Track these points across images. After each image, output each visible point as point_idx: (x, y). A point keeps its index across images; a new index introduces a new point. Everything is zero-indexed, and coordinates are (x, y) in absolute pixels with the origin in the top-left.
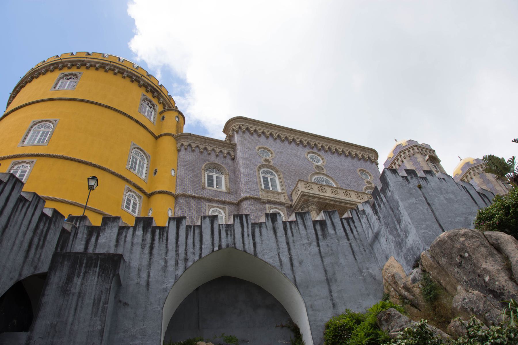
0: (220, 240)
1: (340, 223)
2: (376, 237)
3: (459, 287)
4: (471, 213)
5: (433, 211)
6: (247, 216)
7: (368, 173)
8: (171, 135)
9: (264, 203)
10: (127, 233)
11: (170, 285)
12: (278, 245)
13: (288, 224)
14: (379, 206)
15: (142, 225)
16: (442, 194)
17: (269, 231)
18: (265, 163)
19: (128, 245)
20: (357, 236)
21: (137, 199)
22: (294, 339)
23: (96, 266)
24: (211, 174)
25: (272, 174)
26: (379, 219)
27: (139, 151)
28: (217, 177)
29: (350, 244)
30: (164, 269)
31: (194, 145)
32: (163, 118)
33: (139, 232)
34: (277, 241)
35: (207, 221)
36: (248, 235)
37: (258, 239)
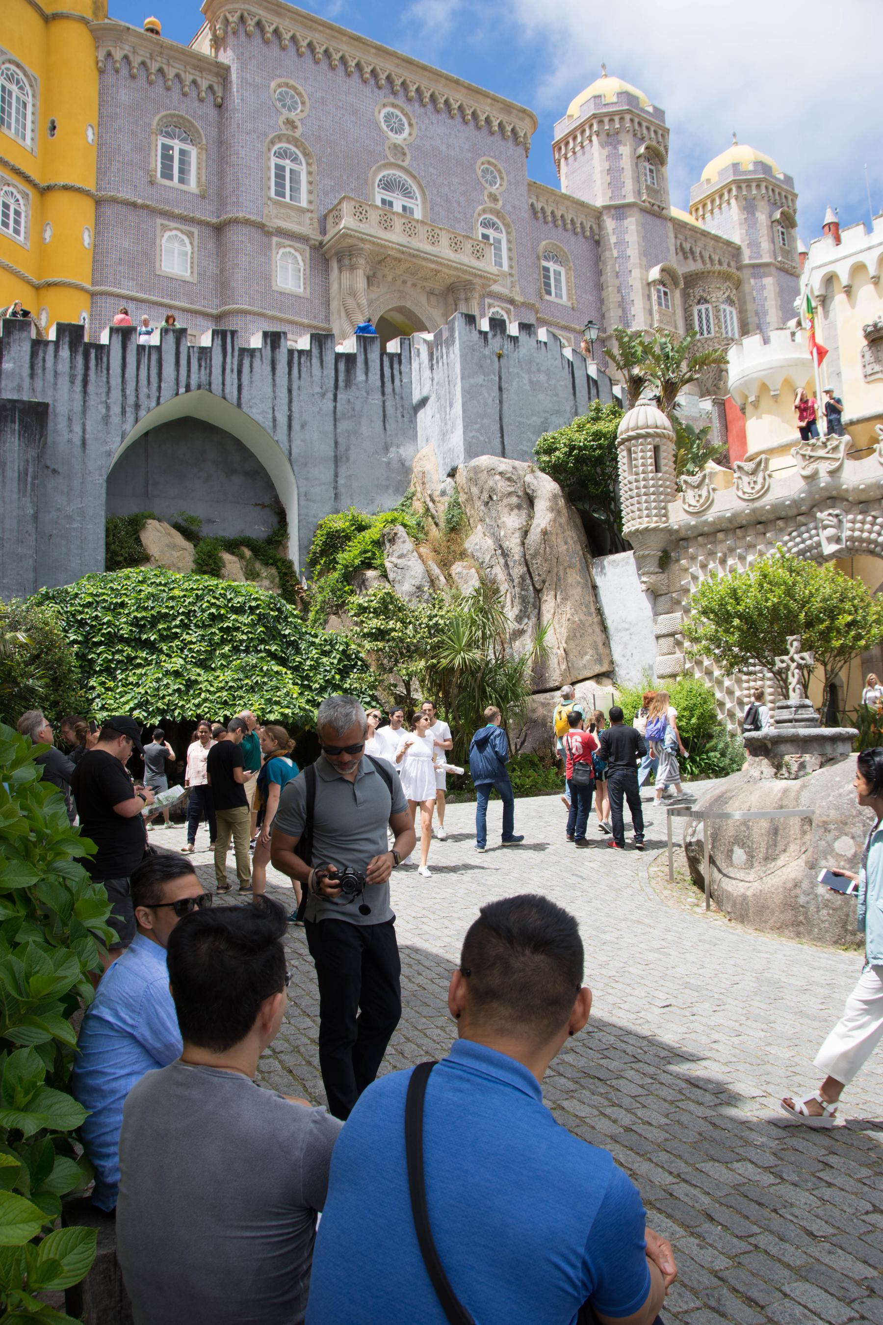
2: (424, 402)
3: (479, 527)
4: (558, 412)
5: (501, 402)
6: (233, 333)
10: (45, 353)
11: (114, 446)
12: (274, 392)
13: (296, 355)
14: (438, 362)
15: (67, 339)
16: (529, 372)
17: (264, 366)
18: (285, 130)
19: (50, 376)
20: (397, 390)
22: (276, 526)
23: (13, 422)
24: (168, 142)
25: (295, 160)
26: (433, 380)
28: (182, 152)
29: (384, 402)
30: (106, 419)
33: (65, 353)
34: (274, 385)
35: (171, 338)
36: (232, 370)
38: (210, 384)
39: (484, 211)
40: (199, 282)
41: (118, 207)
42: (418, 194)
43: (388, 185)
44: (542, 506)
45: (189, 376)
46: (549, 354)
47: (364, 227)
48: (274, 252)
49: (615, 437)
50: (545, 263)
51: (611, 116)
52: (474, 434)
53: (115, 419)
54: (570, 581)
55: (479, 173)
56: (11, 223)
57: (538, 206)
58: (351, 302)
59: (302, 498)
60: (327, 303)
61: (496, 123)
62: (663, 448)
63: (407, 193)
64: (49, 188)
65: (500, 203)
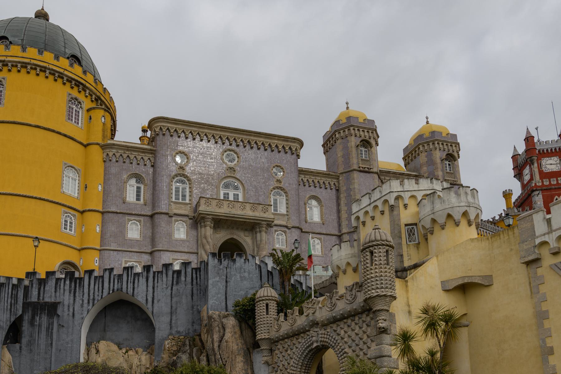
5: (226, 287)
8: (98, 144)
13: (156, 273)
16: (240, 273)
31: (118, 155)
32: (91, 118)
34: (147, 286)
37: (136, 285)
38: (122, 288)
39: (274, 189)
43: (227, 186)
44: (228, 330)
45: (114, 286)
52: (214, 301)
54: (237, 361)
57: (305, 180)
58: (204, 241)
62: (270, 304)
63: (236, 188)
65: (282, 183)
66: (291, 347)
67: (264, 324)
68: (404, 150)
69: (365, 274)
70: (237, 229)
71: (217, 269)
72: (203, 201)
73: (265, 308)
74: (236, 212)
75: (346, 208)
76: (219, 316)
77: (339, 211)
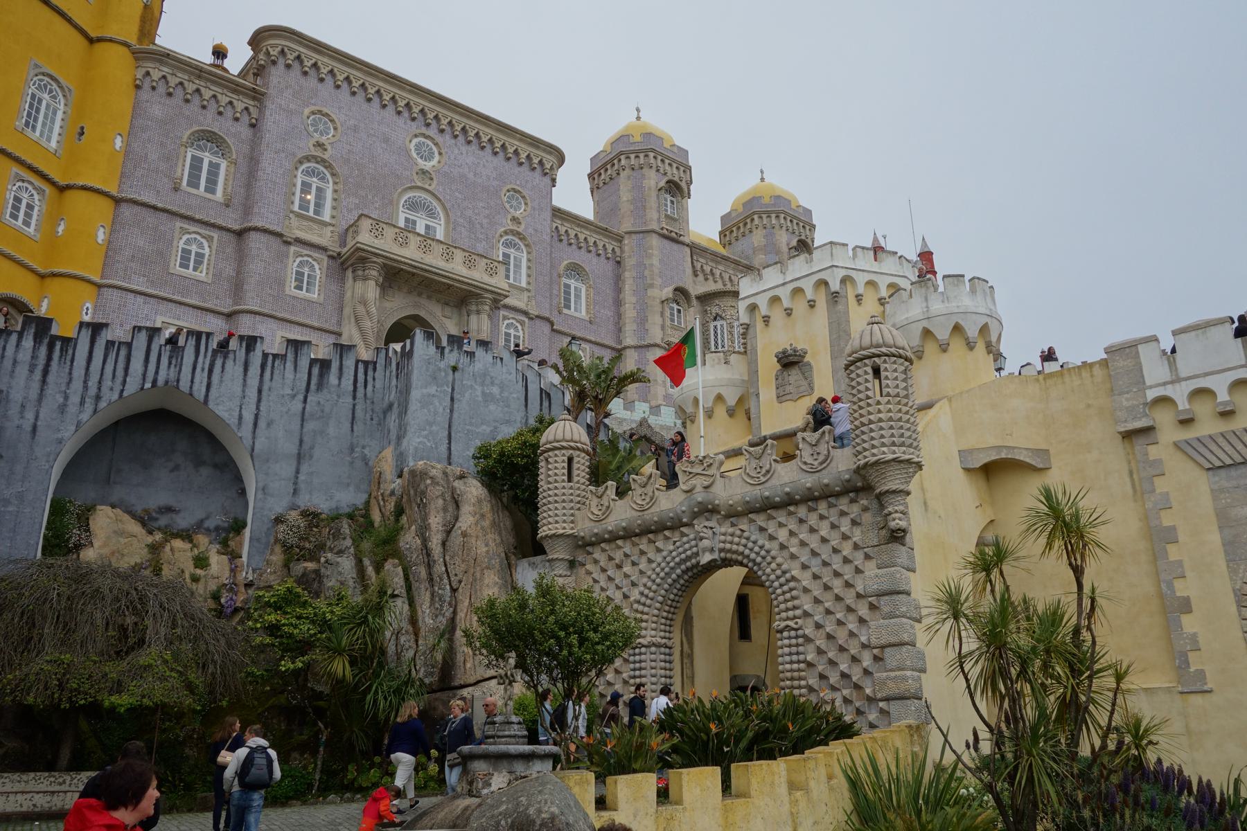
0: (157, 373)
1: (353, 368)
4: (508, 422)
5: (452, 411)
7: (523, 197)
9: (289, 243)
10: (6, 342)
11: (67, 435)
13: (270, 358)
16: (483, 384)
21: (36, 197)
24: (199, 154)
25: (323, 179)
27: (46, 79)
29: (354, 406)
30: (62, 408)
31: (173, 81)
33: (28, 343)
36: (203, 370)
39: (506, 233)
40: (214, 282)
41: (137, 209)
42: (442, 215)
43: (413, 206)
44: (466, 509)
46: (504, 370)
47: (378, 243)
48: (291, 260)
49: (539, 447)
50: (564, 280)
51: (637, 153)
53: (72, 409)
54: (486, 582)
55: (505, 199)
56: (21, 215)
57: (562, 230)
58: (361, 309)
59: (260, 492)
60: (341, 309)
61: (523, 156)
63: (431, 214)
64: (69, 187)
65: (523, 226)
66: (634, 558)
67: (556, 502)
68: (724, 219)
69: (856, 415)
70: (429, 298)
71: (431, 367)
72: (365, 224)
73: (566, 465)
74: (434, 262)
75: (634, 300)
76: (445, 473)
77: (618, 303)
